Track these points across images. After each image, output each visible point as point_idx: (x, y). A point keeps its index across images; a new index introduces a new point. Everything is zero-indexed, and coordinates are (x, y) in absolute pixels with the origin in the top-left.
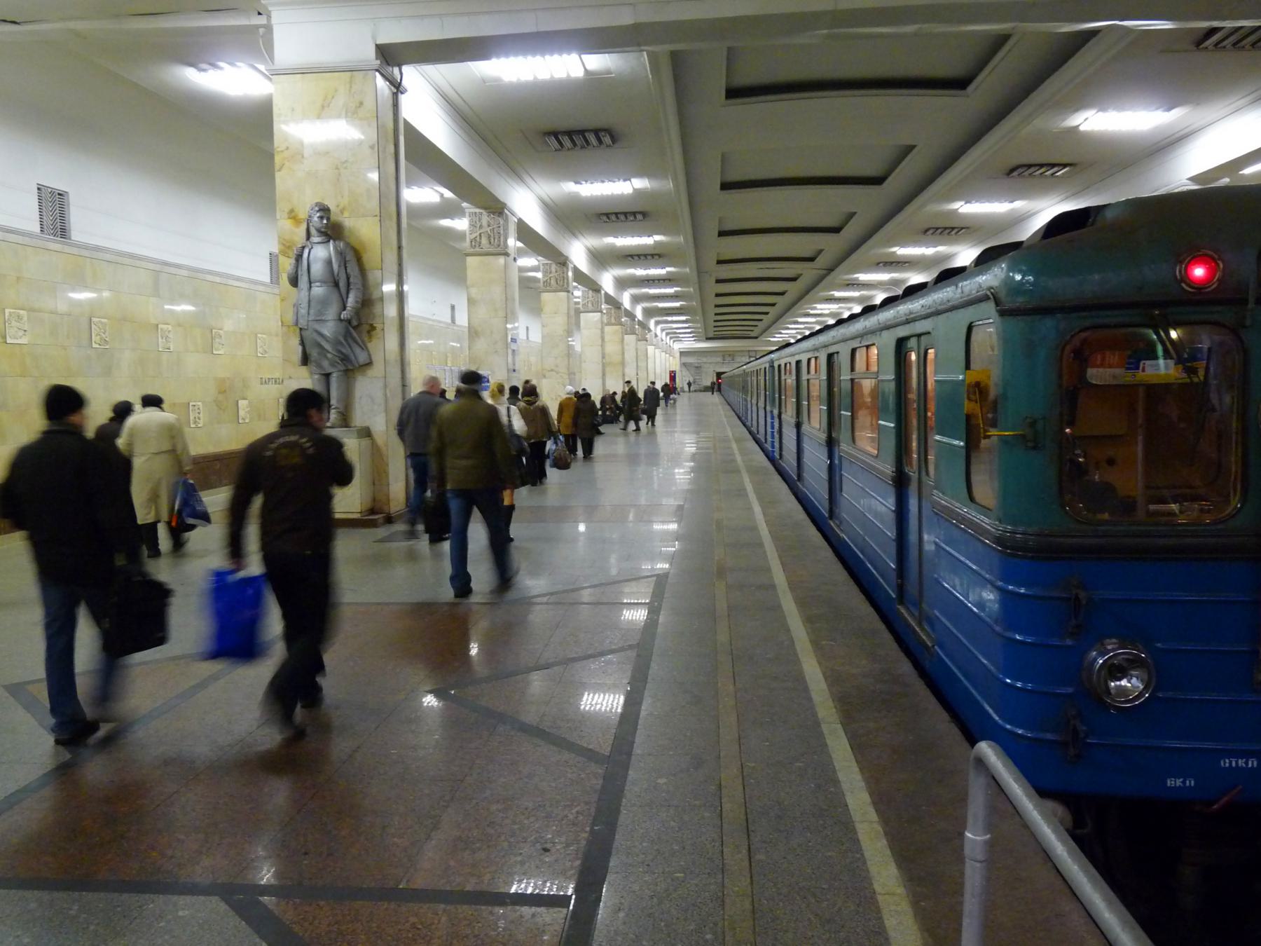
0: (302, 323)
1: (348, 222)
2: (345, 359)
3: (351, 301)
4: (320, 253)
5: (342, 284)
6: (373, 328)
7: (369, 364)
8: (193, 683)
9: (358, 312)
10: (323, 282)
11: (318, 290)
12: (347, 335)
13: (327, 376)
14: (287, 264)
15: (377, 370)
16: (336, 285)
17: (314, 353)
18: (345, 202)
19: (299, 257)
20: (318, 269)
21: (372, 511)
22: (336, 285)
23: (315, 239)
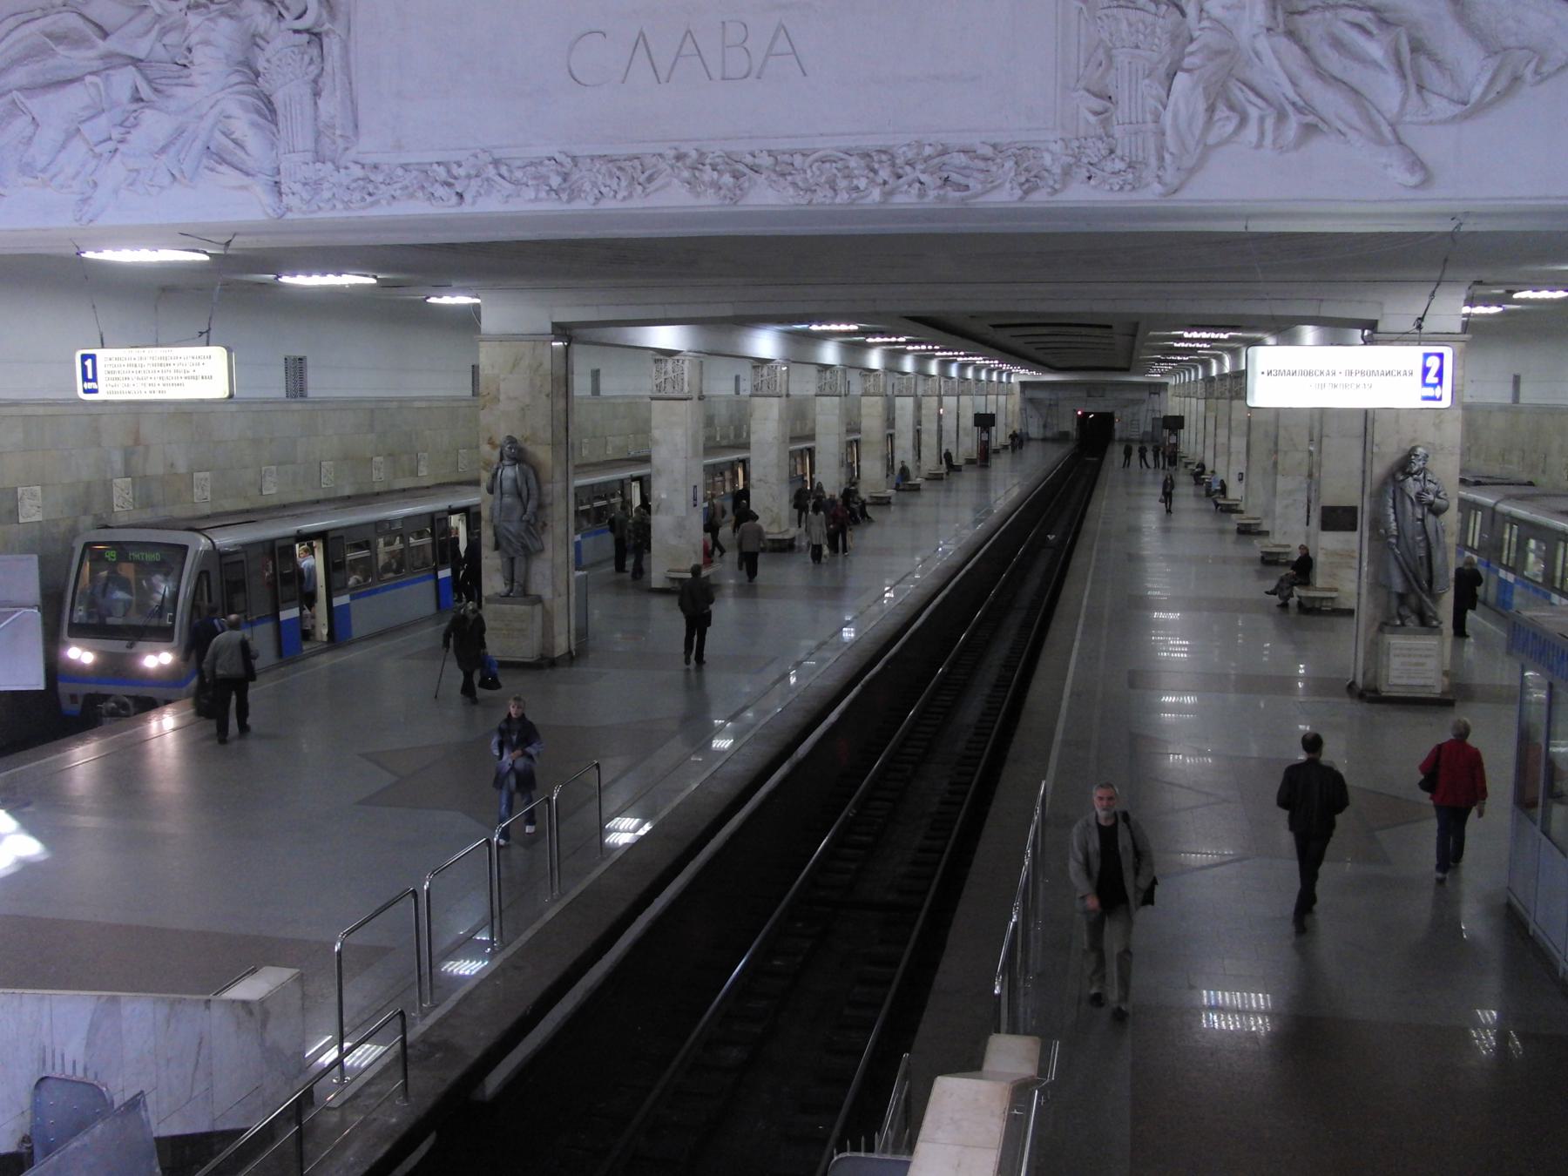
0: (496, 521)
1: (529, 447)
2: (525, 547)
3: (531, 506)
4: (509, 472)
5: (524, 494)
6: (545, 525)
7: (542, 550)
9: (535, 515)
11: (508, 500)
12: (527, 531)
13: (512, 560)
15: (548, 554)
16: (520, 495)
17: (504, 543)
19: (494, 476)
20: (507, 484)
22: (520, 495)
23: (506, 462)
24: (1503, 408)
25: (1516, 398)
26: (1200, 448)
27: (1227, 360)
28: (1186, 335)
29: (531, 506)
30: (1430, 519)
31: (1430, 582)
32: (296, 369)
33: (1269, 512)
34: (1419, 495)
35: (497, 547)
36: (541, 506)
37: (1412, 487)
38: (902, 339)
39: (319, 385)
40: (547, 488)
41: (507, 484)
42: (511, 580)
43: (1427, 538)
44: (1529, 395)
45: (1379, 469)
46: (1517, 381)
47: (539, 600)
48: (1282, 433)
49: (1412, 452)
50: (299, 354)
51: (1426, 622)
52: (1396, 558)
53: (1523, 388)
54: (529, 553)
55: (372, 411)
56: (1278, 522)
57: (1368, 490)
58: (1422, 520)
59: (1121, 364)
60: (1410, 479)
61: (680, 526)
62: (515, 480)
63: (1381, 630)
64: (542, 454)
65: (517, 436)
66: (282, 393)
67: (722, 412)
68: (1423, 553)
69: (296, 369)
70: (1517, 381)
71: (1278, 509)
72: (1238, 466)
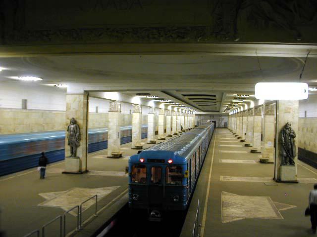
1: (77, 120)
2: (76, 145)
3: (78, 134)
7: (80, 145)
8: (56, 200)
10: (73, 131)
14: (67, 127)
15: (81, 147)
16: (75, 131)
18: (77, 117)
20: (72, 129)
21: (79, 171)
24: (302, 118)
25: (306, 116)
26: (235, 128)
27: (242, 107)
28: (233, 101)
29: (78, 134)
30: (292, 139)
31: (292, 153)
32: (25, 102)
33: (252, 141)
34: (289, 133)
35: (69, 144)
36: (80, 135)
37: (288, 131)
38: (169, 101)
39: (30, 106)
40: (81, 130)
41: (72, 129)
42: (72, 153)
43: (291, 144)
44: (308, 115)
45: (280, 127)
46: (306, 112)
47: (79, 158)
48: (255, 122)
49: (287, 123)
50: (26, 98)
51: (292, 163)
52: (284, 148)
53: (307, 114)
54: (77, 146)
55: (43, 113)
56: (255, 143)
57: (277, 132)
58: (290, 139)
59: (218, 110)
60: (287, 130)
61: (115, 142)
62: (74, 128)
63: (281, 165)
64: (81, 122)
65: (75, 118)
66: (21, 108)
67: (127, 117)
68: (290, 147)
69: (25, 102)
70: (306, 112)
71: (255, 140)
72: (244, 131)
